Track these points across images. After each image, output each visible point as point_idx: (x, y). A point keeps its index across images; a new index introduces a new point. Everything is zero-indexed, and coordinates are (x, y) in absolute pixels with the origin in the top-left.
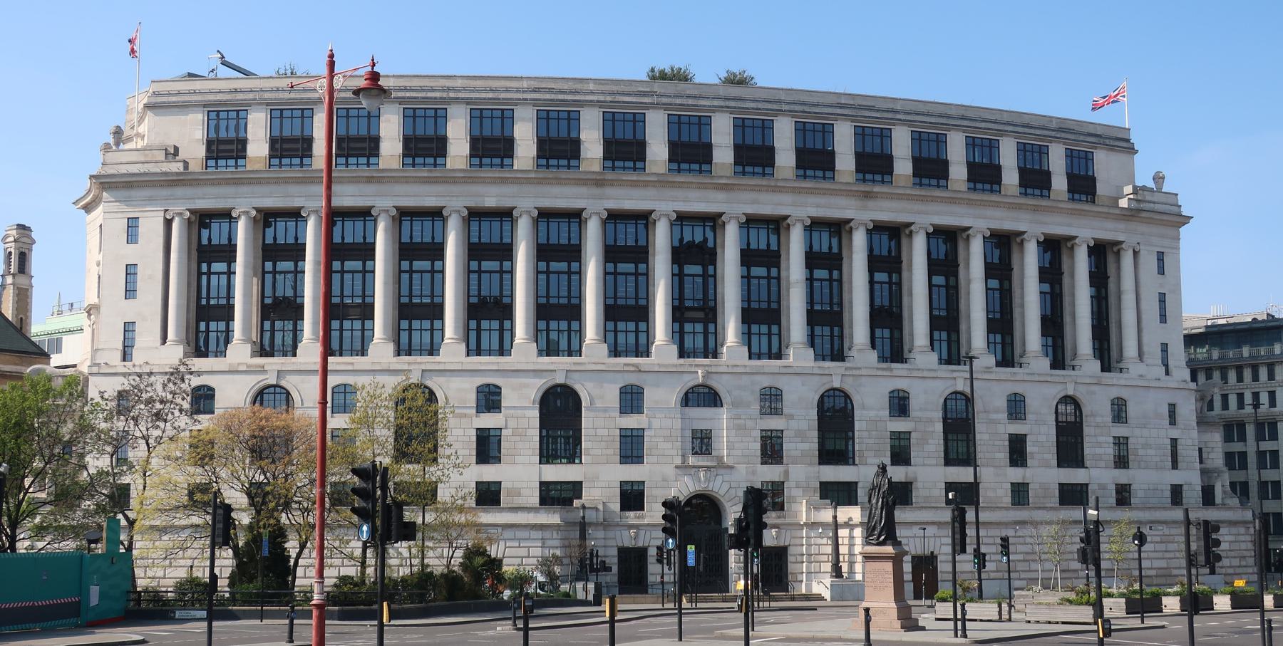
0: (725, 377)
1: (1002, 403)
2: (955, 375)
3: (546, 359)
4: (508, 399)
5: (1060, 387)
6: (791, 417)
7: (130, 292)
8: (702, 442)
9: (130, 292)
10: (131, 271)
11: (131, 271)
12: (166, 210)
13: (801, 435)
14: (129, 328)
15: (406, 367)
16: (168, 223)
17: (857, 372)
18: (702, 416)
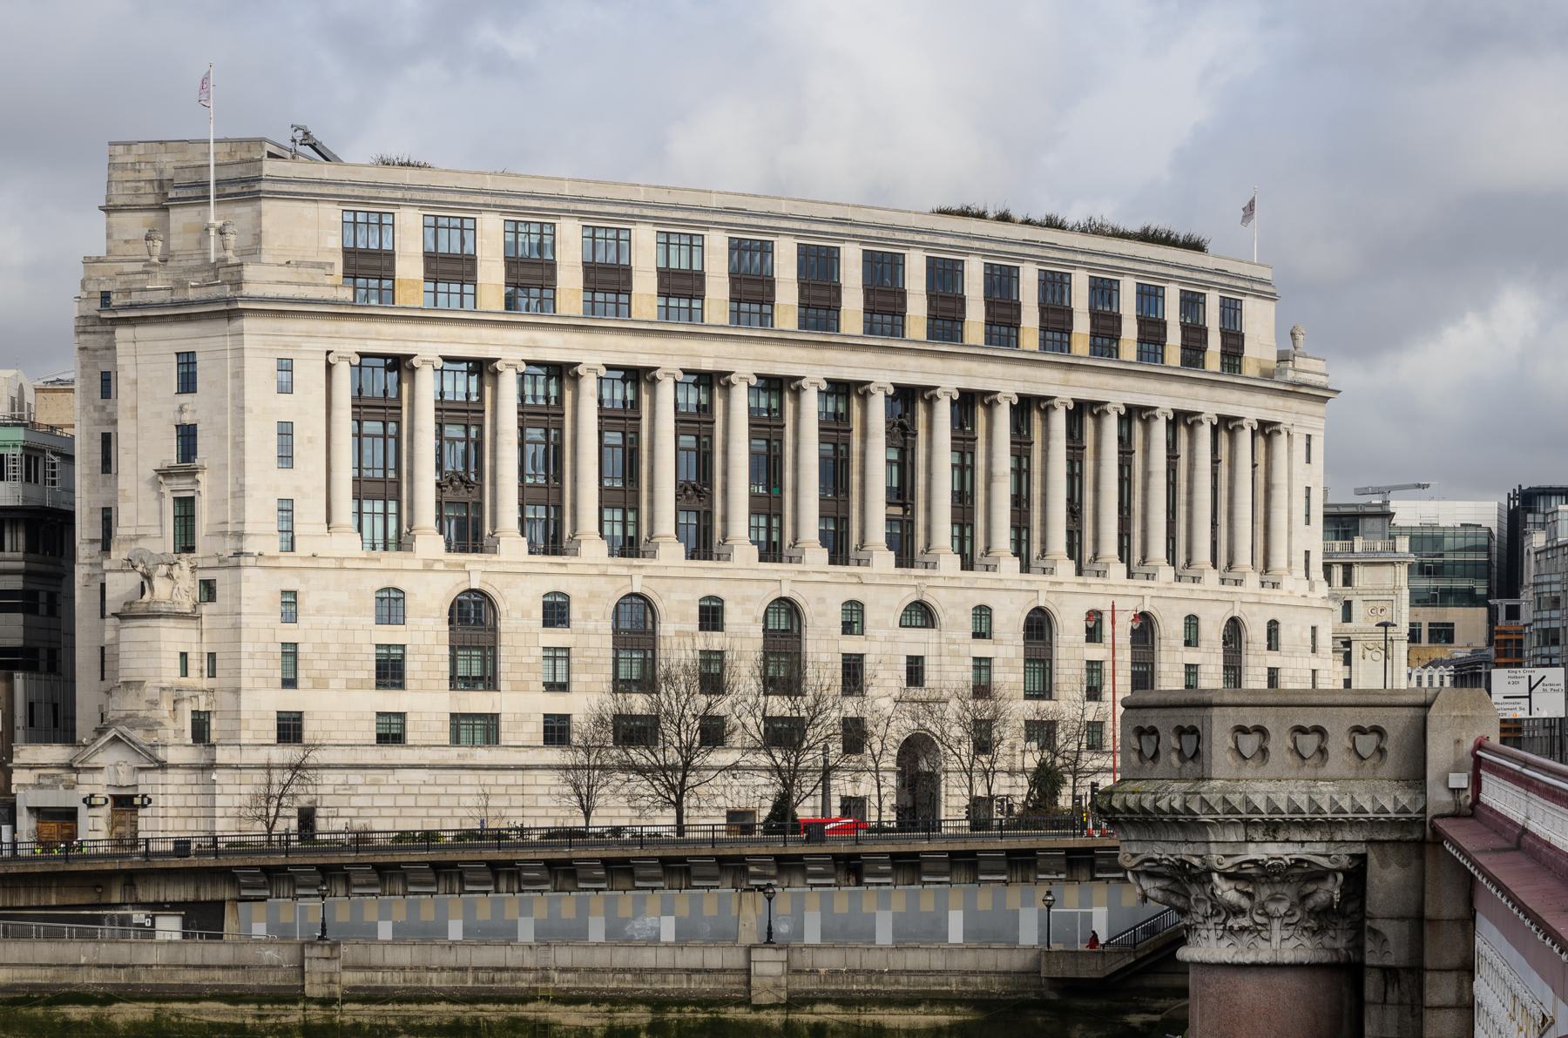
0: (942, 592)
1: (1179, 627)
2: (1143, 592)
3: (768, 565)
4: (731, 616)
5: (1228, 606)
6: (1000, 642)
7: (286, 458)
8: (915, 670)
9: (286, 458)
10: (286, 432)
11: (286, 432)
12: (328, 353)
13: (1008, 662)
14: (286, 509)
15: (625, 571)
16: (329, 367)
17: (1058, 588)
18: (918, 641)
